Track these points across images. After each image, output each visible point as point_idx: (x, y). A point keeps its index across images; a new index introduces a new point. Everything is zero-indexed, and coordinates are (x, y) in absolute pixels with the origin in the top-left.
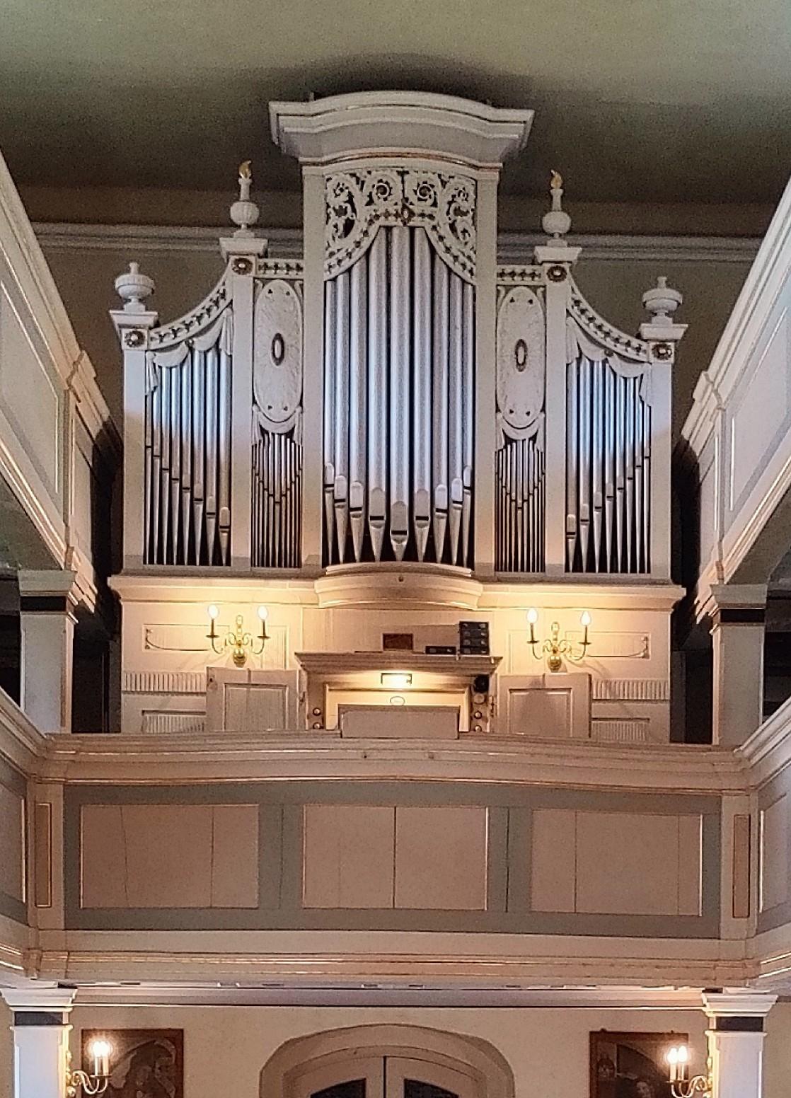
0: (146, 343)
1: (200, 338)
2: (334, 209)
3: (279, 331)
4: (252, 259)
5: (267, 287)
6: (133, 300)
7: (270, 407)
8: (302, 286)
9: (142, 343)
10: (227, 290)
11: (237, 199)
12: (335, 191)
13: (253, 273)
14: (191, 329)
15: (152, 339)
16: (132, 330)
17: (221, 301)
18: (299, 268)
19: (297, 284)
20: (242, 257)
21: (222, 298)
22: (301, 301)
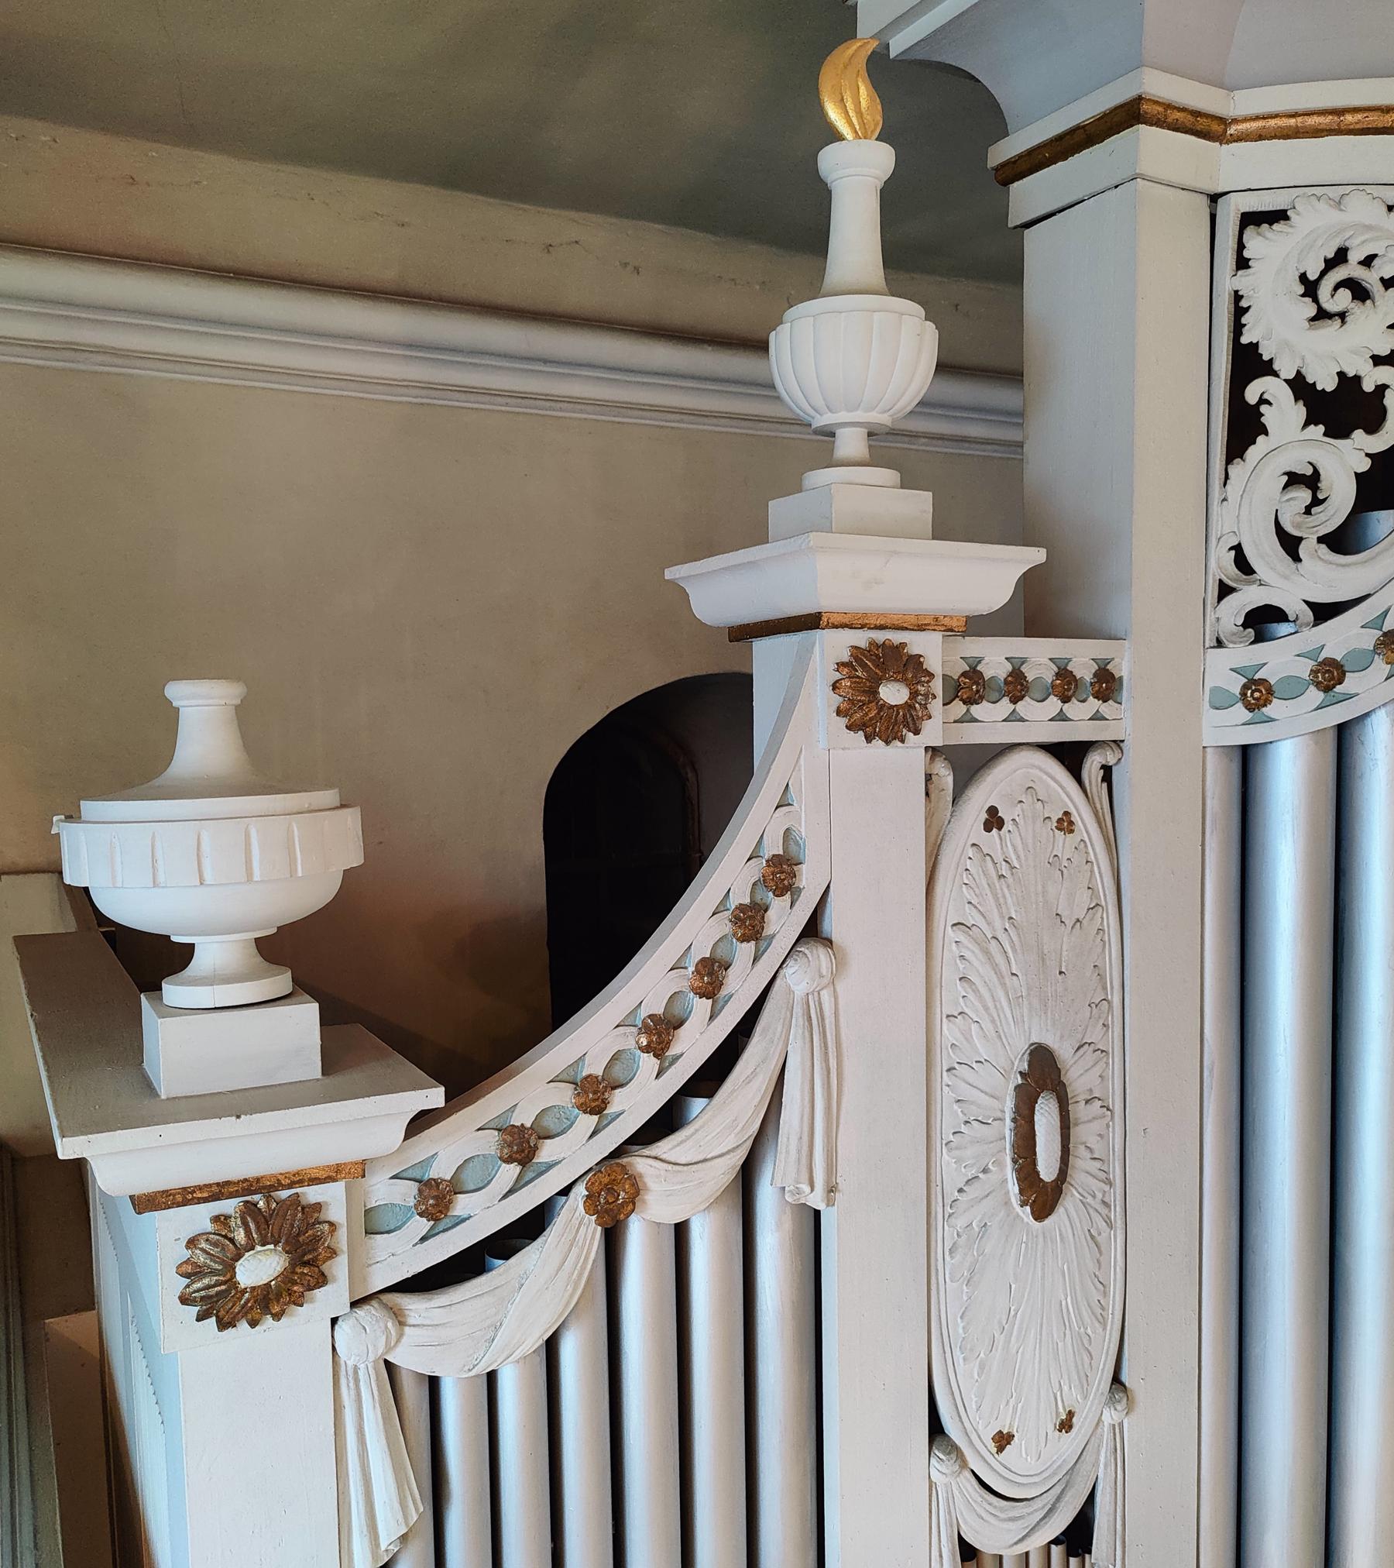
0: (339, 1268)
1: (664, 1147)
2: (1300, 386)
3: (1035, 1039)
4: (928, 646)
5: (983, 794)
6: (202, 962)
7: (1003, 1440)
8: (1107, 772)
9: (322, 1280)
10: (803, 830)
11: (814, 287)
12: (1310, 288)
13: (933, 732)
14: (618, 1101)
15: (373, 1224)
16: (229, 1206)
17: (778, 906)
18: (1106, 684)
19: (1092, 765)
20: (880, 636)
21: (779, 892)
22: (1112, 846)
